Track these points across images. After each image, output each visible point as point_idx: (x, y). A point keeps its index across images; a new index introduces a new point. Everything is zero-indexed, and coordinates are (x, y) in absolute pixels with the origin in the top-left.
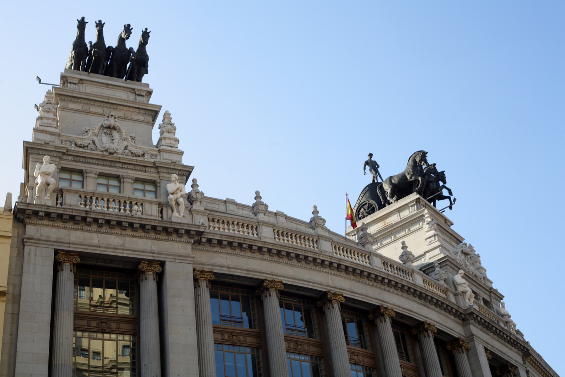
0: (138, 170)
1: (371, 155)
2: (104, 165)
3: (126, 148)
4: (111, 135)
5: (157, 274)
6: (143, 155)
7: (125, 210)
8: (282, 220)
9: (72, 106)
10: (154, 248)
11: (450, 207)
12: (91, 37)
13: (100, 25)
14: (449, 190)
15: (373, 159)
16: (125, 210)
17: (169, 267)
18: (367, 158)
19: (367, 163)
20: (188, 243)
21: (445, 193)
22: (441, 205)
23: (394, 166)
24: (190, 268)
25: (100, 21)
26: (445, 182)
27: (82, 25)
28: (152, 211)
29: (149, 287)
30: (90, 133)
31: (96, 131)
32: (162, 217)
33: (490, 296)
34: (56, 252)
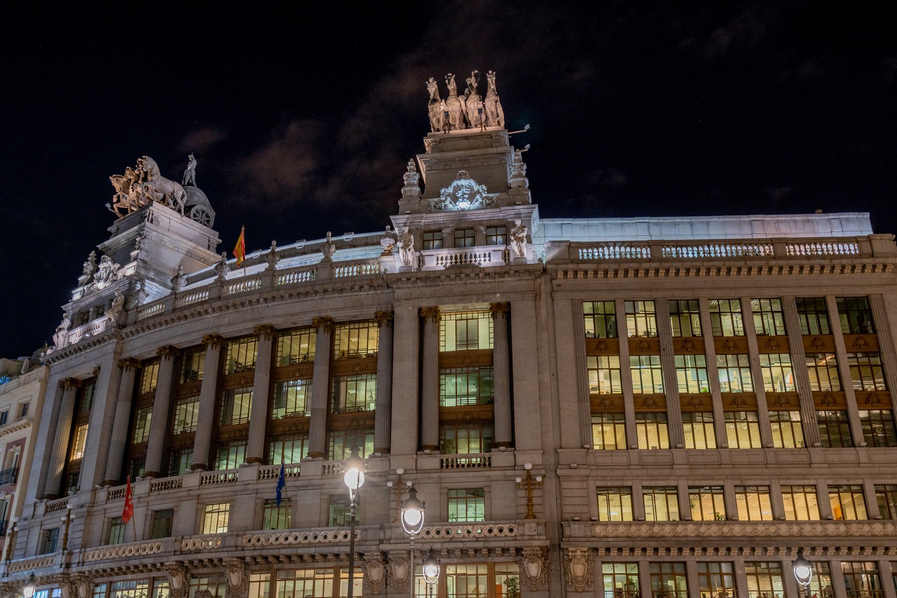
5: (505, 312)
34: (420, 310)
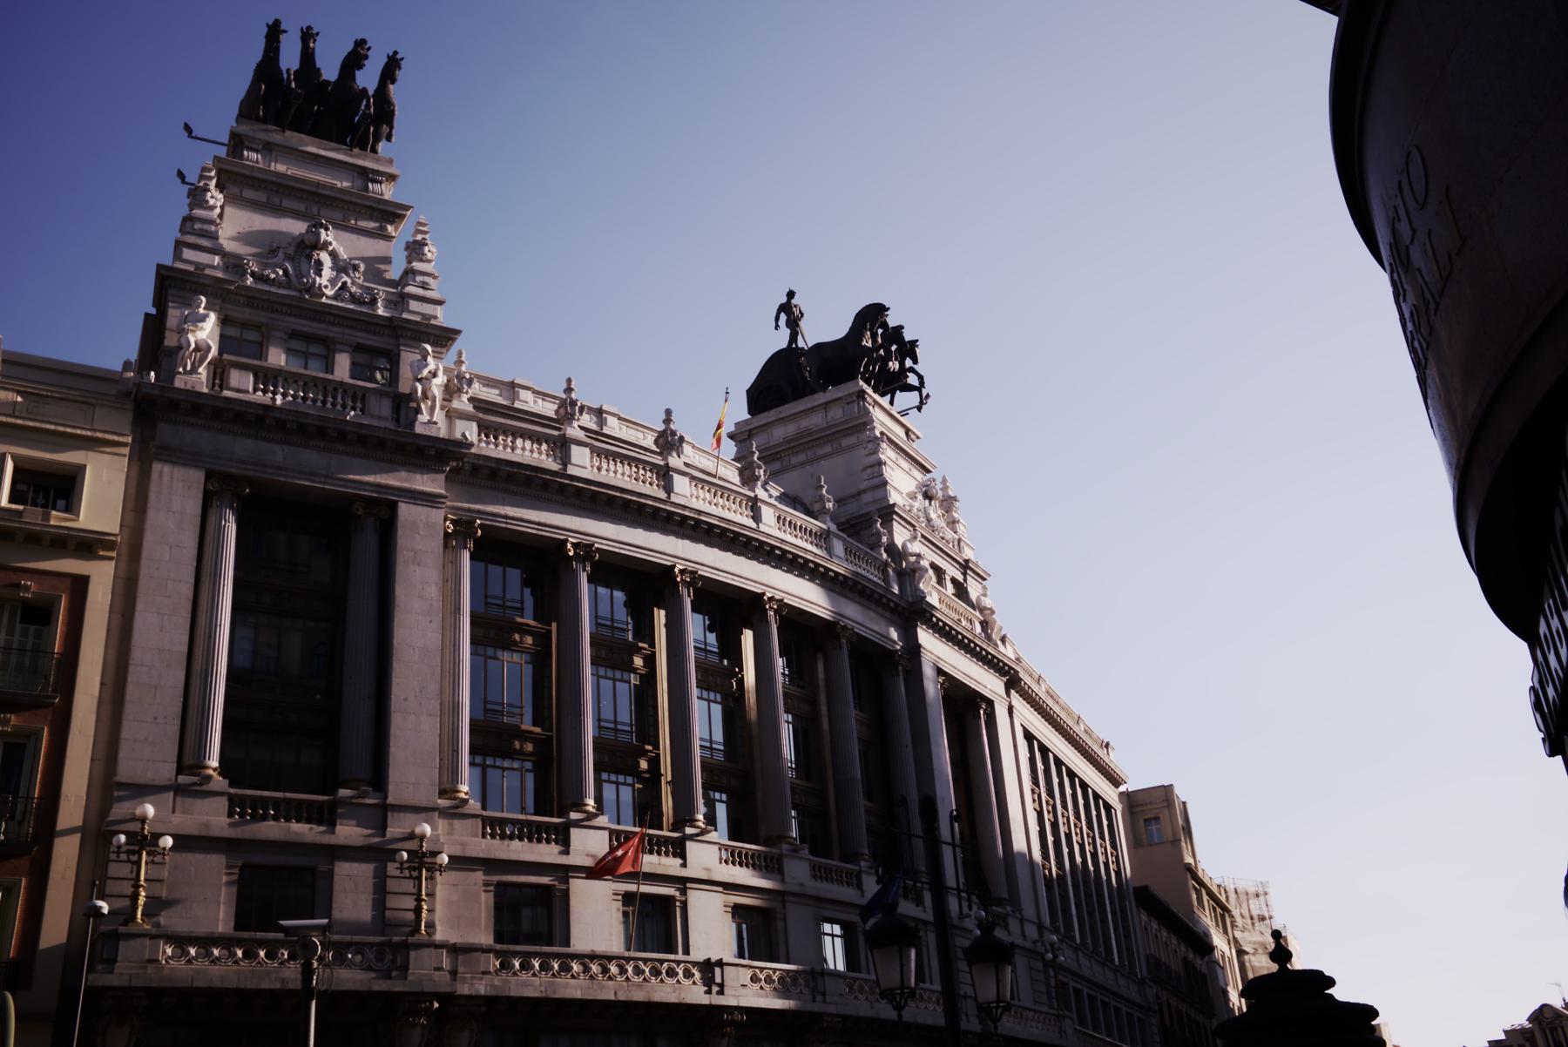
0: (360, 330)
1: (791, 294)
2: (300, 317)
7: (334, 405)
9: (248, 193)
11: (919, 408)
12: (290, 59)
13: (307, 35)
14: (920, 377)
16: (334, 405)
18: (784, 300)
21: (912, 379)
22: (905, 399)
23: (825, 325)
25: (309, 28)
26: (915, 361)
27: (274, 32)
29: (367, 542)
30: (281, 254)
31: (291, 251)
32: (398, 421)
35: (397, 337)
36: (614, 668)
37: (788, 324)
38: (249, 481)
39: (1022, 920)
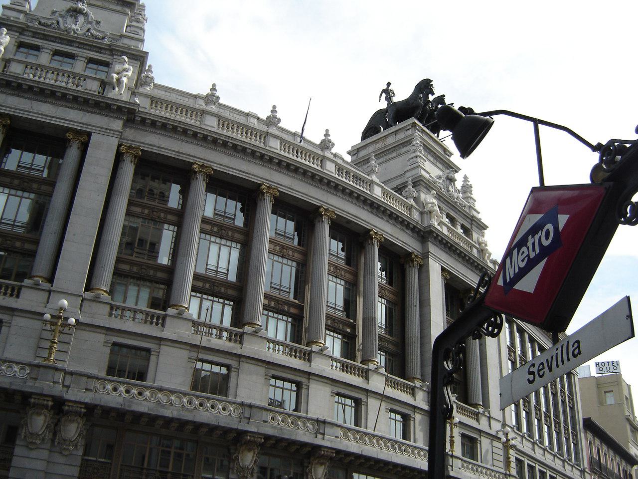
1: (389, 84)
3: (88, 30)
4: (76, 18)
5: (82, 143)
6: (103, 38)
8: (255, 121)
10: (84, 120)
15: (390, 88)
17: (94, 138)
18: (385, 87)
19: (384, 91)
20: (119, 119)
23: (402, 93)
24: (115, 142)
28: (93, 87)
30: (57, 14)
33: (472, 224)
35: (113, 55)
36: (221, 238)
37: (386, 99)
38: (11, 117)
39: (489, 418)
